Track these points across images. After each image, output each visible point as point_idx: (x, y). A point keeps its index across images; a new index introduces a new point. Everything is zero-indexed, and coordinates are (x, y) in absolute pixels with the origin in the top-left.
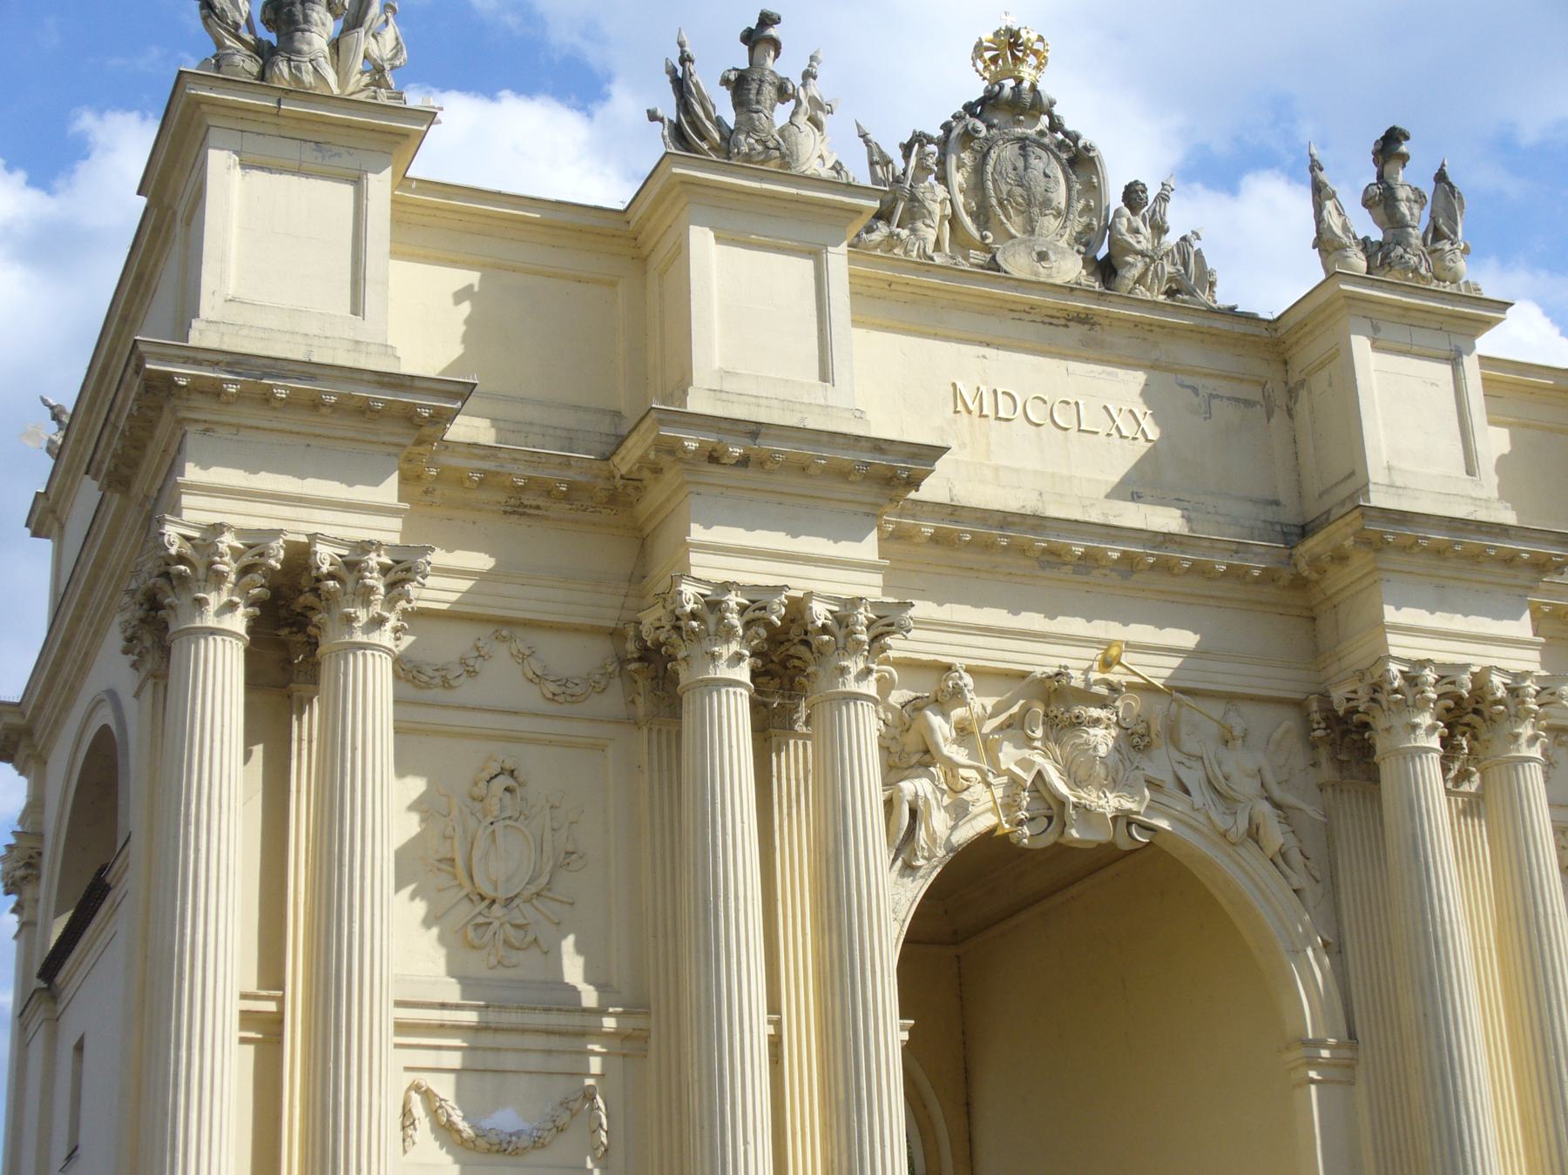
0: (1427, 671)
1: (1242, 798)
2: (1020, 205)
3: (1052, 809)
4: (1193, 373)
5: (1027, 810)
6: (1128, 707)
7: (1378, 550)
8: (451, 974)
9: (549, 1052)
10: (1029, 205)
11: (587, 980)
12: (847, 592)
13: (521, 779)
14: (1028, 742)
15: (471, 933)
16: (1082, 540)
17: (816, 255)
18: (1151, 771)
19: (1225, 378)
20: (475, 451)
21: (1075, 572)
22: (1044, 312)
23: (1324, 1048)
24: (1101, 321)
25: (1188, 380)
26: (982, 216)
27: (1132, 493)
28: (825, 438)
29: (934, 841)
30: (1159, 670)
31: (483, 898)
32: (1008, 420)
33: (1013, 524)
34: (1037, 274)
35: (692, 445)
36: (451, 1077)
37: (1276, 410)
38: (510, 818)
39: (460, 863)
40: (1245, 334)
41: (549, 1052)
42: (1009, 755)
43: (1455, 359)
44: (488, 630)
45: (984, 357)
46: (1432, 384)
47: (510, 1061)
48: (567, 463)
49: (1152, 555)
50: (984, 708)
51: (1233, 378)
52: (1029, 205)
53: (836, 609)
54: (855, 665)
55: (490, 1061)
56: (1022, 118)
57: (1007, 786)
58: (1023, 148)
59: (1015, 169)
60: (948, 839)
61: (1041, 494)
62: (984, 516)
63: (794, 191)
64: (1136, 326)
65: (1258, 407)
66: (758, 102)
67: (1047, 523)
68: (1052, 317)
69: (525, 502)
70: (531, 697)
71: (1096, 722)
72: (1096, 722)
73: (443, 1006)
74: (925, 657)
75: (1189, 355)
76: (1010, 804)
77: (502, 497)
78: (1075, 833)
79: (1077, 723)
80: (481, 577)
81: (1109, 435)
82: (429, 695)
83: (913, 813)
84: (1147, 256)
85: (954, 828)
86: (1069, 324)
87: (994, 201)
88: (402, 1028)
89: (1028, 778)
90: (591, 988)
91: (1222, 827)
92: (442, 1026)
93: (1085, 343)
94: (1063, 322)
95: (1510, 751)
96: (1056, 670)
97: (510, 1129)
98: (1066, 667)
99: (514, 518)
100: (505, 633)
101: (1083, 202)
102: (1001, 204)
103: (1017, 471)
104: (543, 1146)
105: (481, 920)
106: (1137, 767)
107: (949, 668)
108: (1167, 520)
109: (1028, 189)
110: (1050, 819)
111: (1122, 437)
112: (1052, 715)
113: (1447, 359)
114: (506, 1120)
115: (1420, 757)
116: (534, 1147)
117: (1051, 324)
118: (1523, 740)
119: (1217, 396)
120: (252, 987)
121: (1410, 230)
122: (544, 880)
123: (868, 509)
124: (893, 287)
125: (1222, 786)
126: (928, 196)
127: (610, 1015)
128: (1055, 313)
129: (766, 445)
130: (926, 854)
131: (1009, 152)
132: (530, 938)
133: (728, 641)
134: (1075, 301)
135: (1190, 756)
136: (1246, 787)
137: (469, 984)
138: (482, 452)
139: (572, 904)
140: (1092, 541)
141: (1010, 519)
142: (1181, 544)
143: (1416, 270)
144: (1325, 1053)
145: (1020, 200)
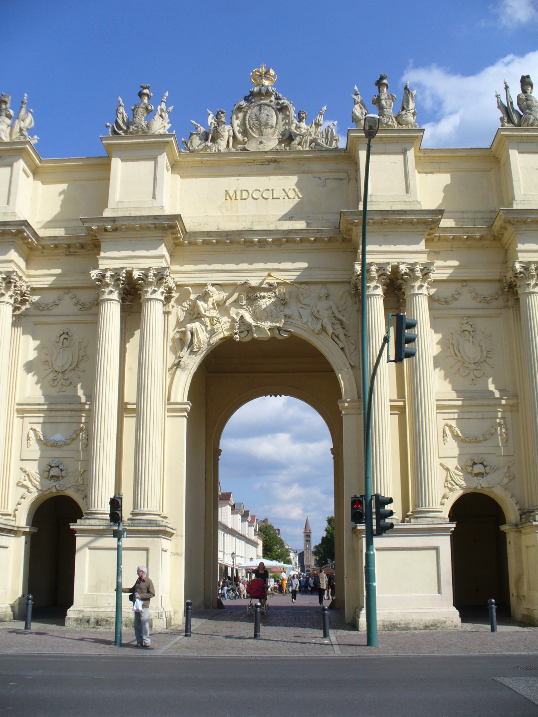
0: (373, 267)
1: (322, 317)
2: (257, 127)
3: (249, 329)
4: (319, 173)
5: (238, 329)
6: (279, 291)
7: (356, 226)
8: (43, 395)
9: (71, 416)
10: (260, 126)
11: (84, 395)
12: (146, 266)
13: (70, 334)
14: (241, 307)
15: (51, 382)
16: (258, 236)
17: (155, 159)
18: (287, 311)
19: (332, 172)
20: (51, 239)
21: (259, 247)
22: (259, 161)
23: (346, 403)
24: (281, 160)
25: (317, 175)
26: (245, 133)
27: (290, 217)
28: (137, 218)
29: (200, 343)
30: (290, 277)
31: (56, 372)
32: (245, 199)
33: (231, 234)
34: (259, 149)
35: (94, 227)
36: (40, 425)
37: (351, 180)
38: (66, 347)
39: (49, 362)
40: (335, 156)
41: (71, 416)
42: (233, 312)
43: (405, 152)
44: (62, 292)
45: (238, 180)
46: (394, 163)
47: (60, 420)
48: (78, 237)
49: (285, 238)
50: (223, 297)
51: (335, 172)
52: (260, 126)
53: (144, 272)
54: (150, 290)
55: (54, 420)
56: (263, 97)
57: (231, 322)
58: (260, 108)
59: (256, 115)
60: (209, 342)
61: (252, 223)
62: (219, 233)
63: (143, 140)
64: (294, 160)
65: (345, 180)
66: (136, 115)
67: (243, 233)
68: (262, 162)
69: (71, 251)
70: (75, 310)
71: (264, 297)
72: (264, 297)
73: (39, 404)
74: (203, 282)
75: (317, 166)
76: (232, 328)
77: (64, 251)
78: (255, 335)
79: (257, 298)
80: (57, 275)
81: (284, 198)
82: (44, 313)
83: (192, 334)
84: (301, 135)
85: (210, 338)
86: (270, 163)
87: (248, 127)
88: (18, 411)
89: (237, 319)
90: (84, 396)
91: (312, 329)
92: (39, 410)
93: (275, 169)
94: (267, 163)
95: (411, 292)
96: (244, 281)
97: (58, 440)
98: (248, 280)
99: (70, 256)
100: (66, 291)
101: (284, 121)
102: (250, 128)
103: (246, 216)
104: (487, 440)
105: (54, 378)
106: (281, 311)
107: (205, 285)
108: (300, 225)
109: (260, 121)
110: (248, 331)
111: (289, 198)
112: (249, 296)
113: (402, 153)
114: (58, 437)
115: (371, 298)
116: (65, 445)
117: (263, 164)
118: (416, 288)
119: (329, 179)
120: (395, 397)
121: (385, 110)
122: (75, 365)
123: (161, 238)
124: (203, 162)
125: (316, 314)
126: (222, 130)
127: (504, 399)
128: (263, 161)
129: (119, 223)
130: (198, 347)
131: (255, 110)
132: (69, 383)
133: (108, 287)
134: (268, 155)
135: (305, 305)
136: (325, 314)
137: (46, 396)
138: (53, 238)
139: (84, 371)
140: (260, 236)
141: (229, 233)
142: (295, 233)
143: (386, 124)
144: (346, 404)
145: (257, 125)
